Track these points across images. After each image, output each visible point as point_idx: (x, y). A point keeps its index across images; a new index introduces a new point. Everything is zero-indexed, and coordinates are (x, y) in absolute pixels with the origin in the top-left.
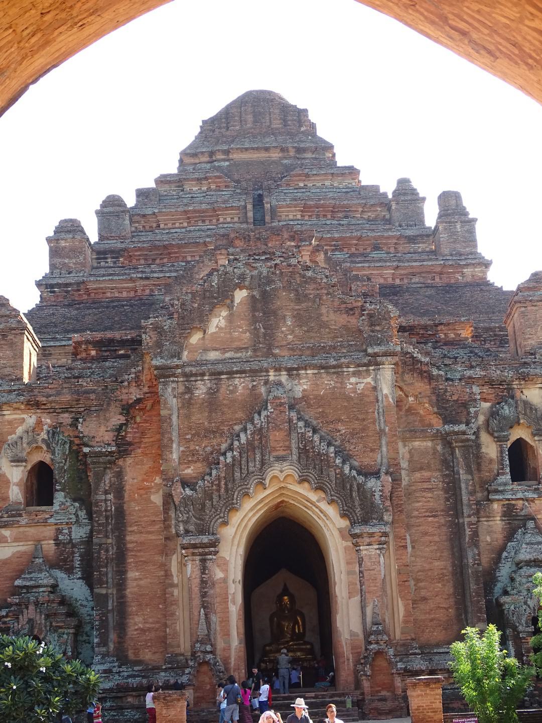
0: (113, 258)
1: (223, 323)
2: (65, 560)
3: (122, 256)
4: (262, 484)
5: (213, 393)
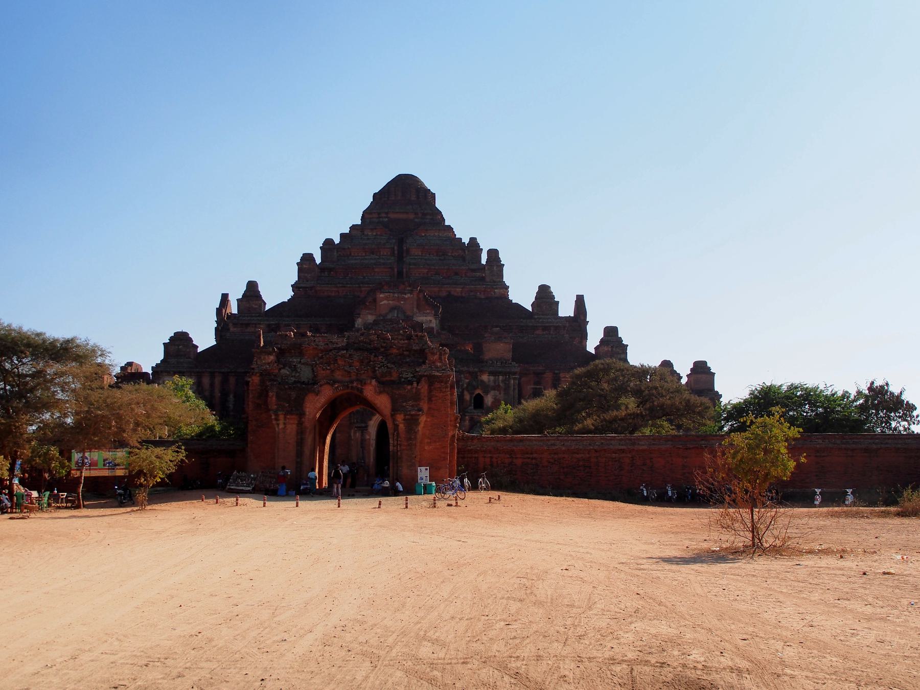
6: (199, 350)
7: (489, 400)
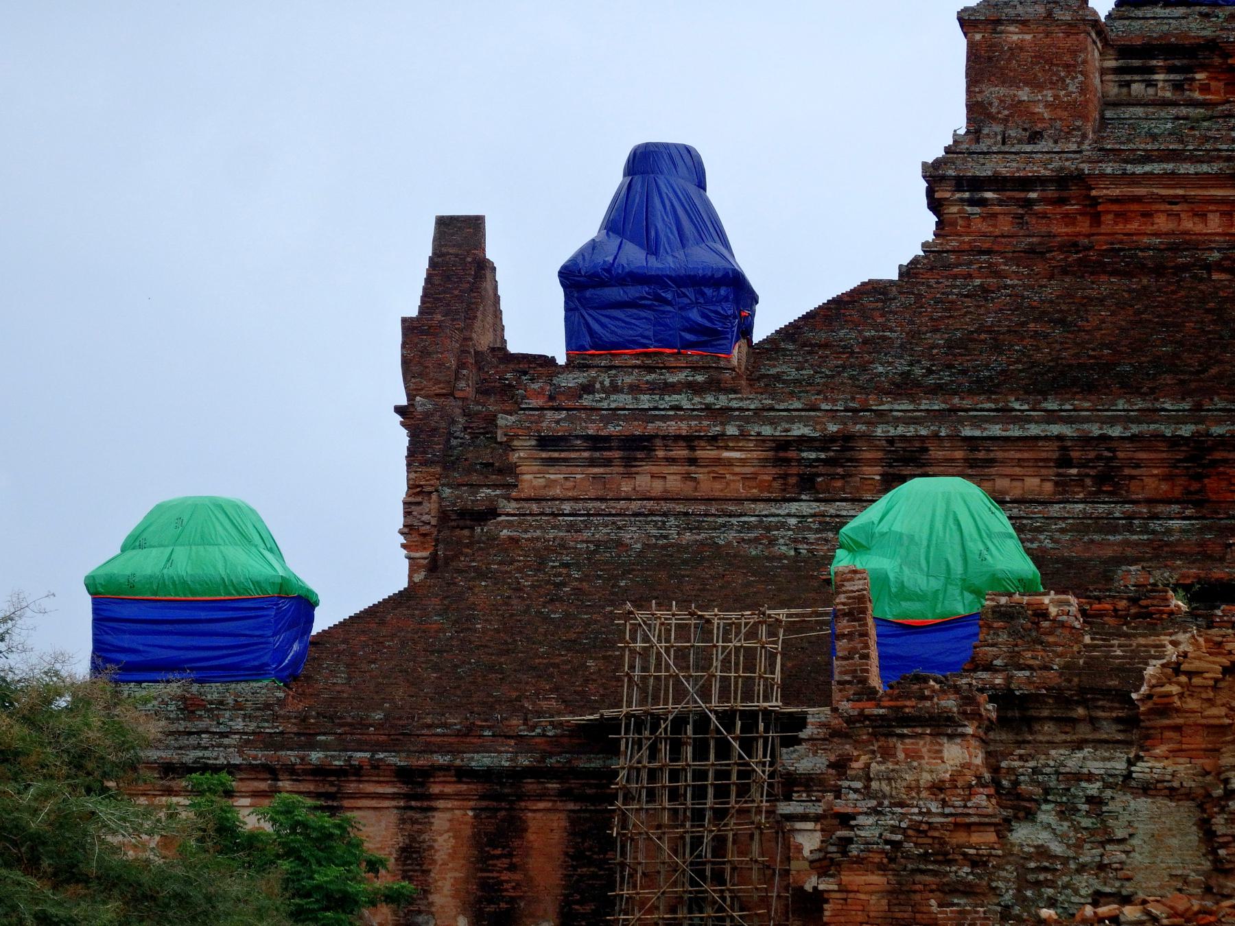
0: (1170, 70)
3: (1203, 68)
6: (322, 621)
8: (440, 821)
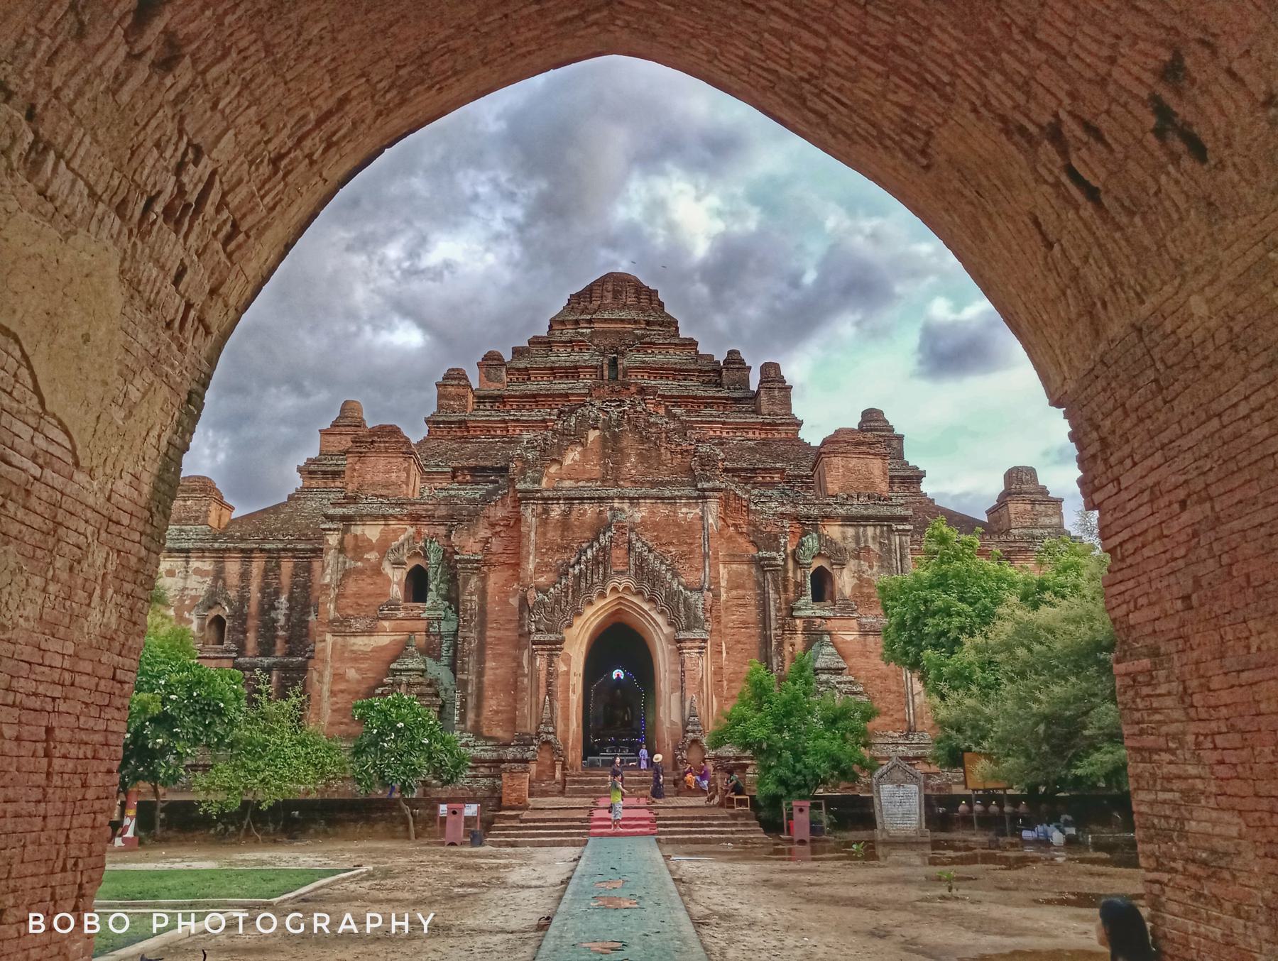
1: (577, 457)
2: (434, 650)
4: (602, 595)
5: (566, 515)
7: (845, 582)
8: (254, 565)
